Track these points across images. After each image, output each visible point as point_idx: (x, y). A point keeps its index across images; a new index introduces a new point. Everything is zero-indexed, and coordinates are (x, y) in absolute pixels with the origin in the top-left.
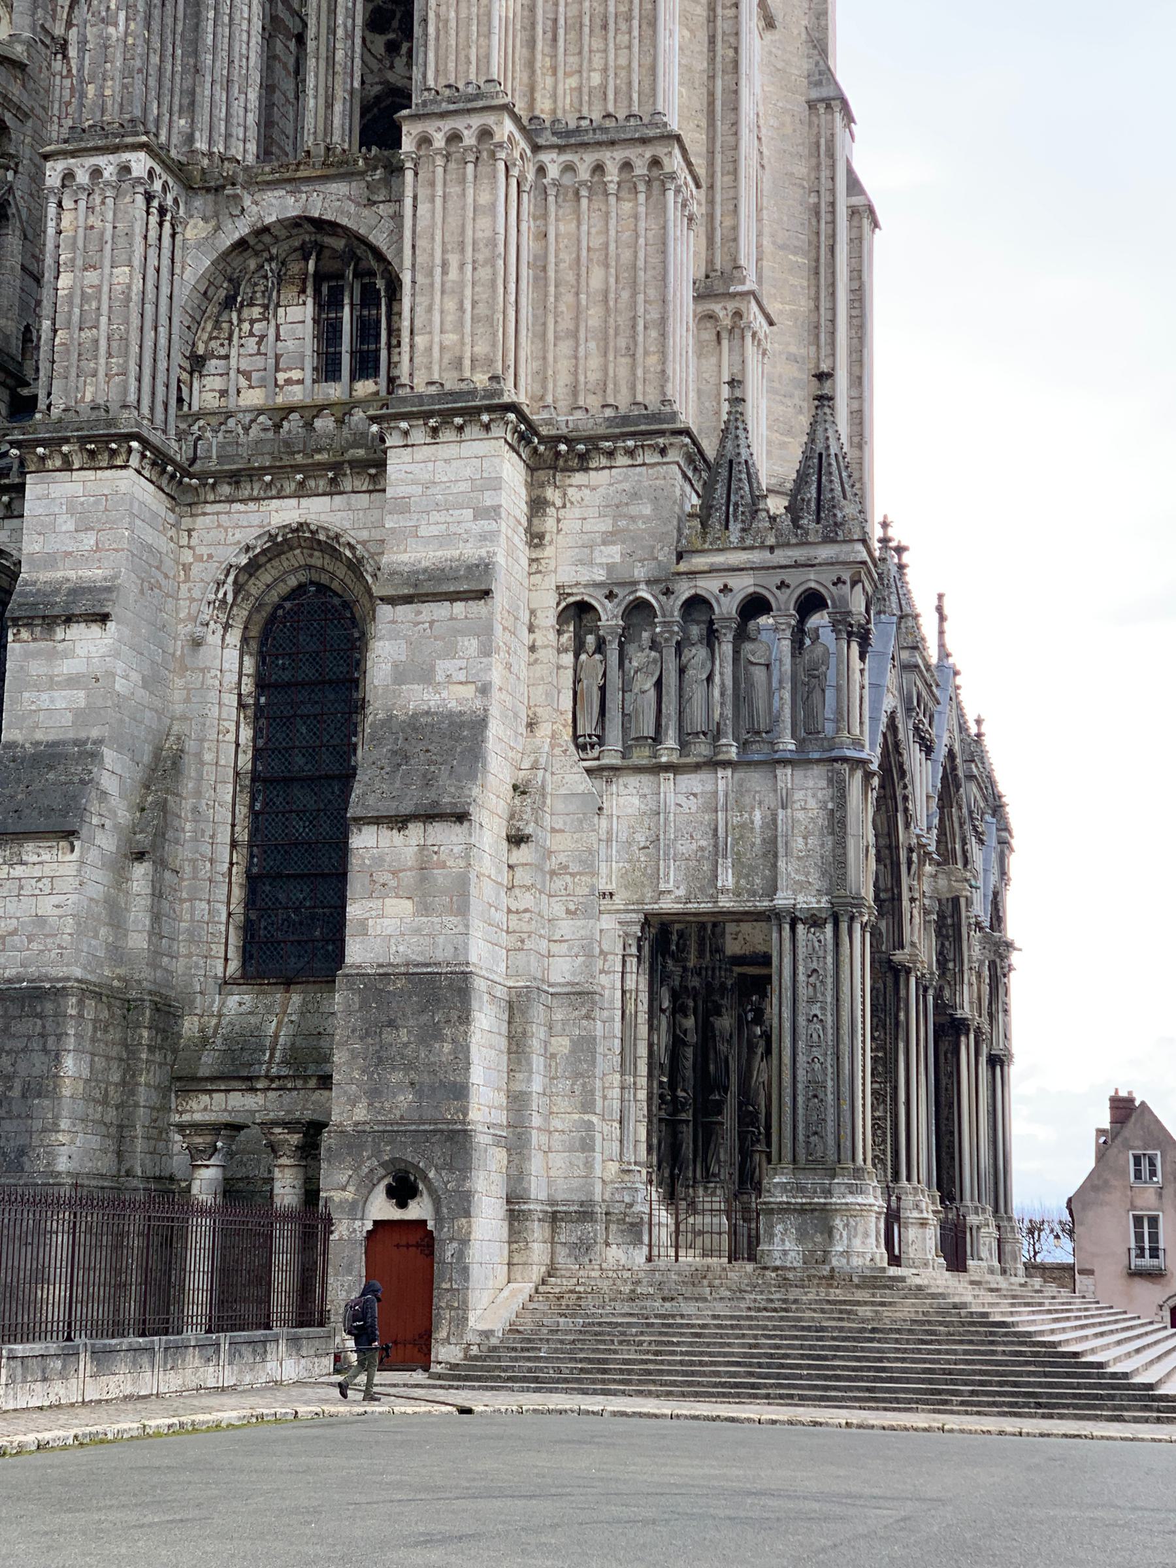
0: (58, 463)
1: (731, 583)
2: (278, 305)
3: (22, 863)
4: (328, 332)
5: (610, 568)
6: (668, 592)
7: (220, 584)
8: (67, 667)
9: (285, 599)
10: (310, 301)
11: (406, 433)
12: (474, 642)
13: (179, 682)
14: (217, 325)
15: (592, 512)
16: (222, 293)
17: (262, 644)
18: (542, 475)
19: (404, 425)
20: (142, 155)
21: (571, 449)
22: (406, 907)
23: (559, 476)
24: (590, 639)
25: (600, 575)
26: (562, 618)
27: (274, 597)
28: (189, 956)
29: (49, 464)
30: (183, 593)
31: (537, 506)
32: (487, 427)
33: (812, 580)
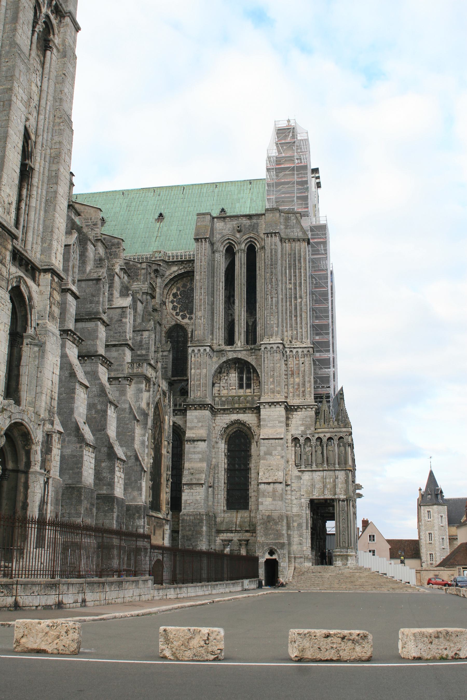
0: (194, 408)
1: (326, 435)
4: (241, 379)
5: (302, 431)
6: (313, 436)
7: (221, 431)
8: (198, 450)
9: (233, 433)
11: (264, 406)
13: (213, 451)
14: (217, 377)
15: (298, 420)
18: (288, 412)
19: (264, 404)
22: (270, 499)
24: (298, 445)
25: (300, 432)
26: (292, 440)
27: (231, 433)
28: (217, 506)
29: (192, 409)
30: (214, 432)
31: (288, 418)
32: (281, 405)
33: (341, 435)
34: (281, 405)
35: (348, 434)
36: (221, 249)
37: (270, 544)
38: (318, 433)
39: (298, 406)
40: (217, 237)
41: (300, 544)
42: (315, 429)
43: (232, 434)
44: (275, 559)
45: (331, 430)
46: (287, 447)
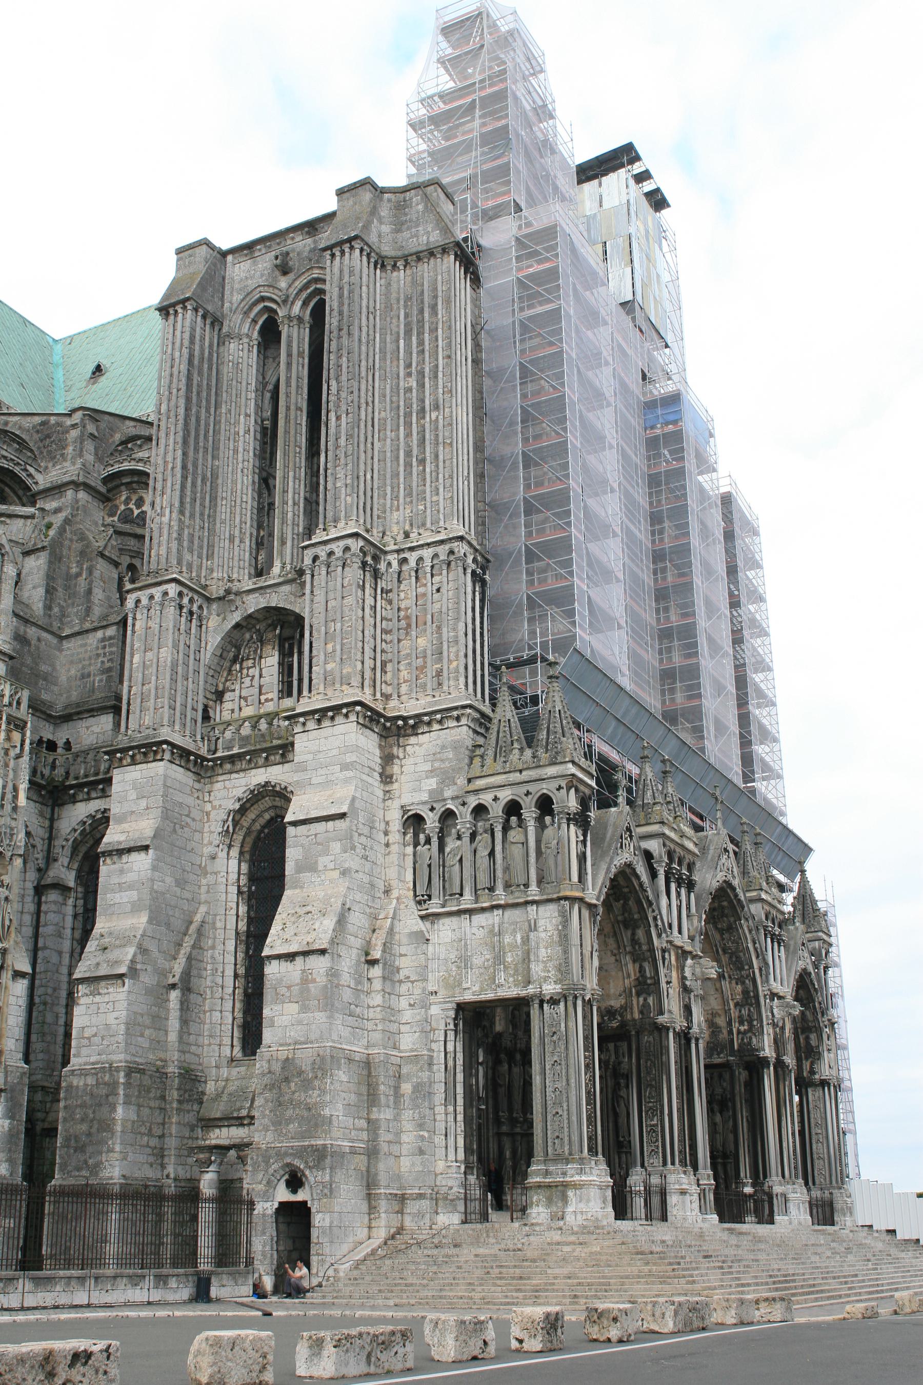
0: (129, 760)
2: (261, 657)
3: (99, 994)
5: (431, 792)
6: (464, 804)
8: (130, 877)
9: (263, 827)
10: (277, 653)
11: (304, 724)
12: (339, 844)
13: (204, 882)
15: (420, 760)
16: (231, 655)
17: (252, 855)
19: (302, 720)
20: (173, 585)
21: (406, 724)
22: (294, 1008)
23: (401, 740)
24: (422, 837)
25: (425, 797)
26: (406, 824)
27: (257, 826)
28: (210, 1045)
29: (125, 762)
31: (388, 759)
33: (545, 788)
34: (346, 716)
35: (563, 784)
36: (245, 329)
37: (286, 1154)
38: (476, 792)
39: (418, 716)
40: (234, 298)
41: (421, 1152)
42: (469, 781)
43: (261, 831)
44: (305, 1203)
45: (515, 777)
46: (387, 845)
